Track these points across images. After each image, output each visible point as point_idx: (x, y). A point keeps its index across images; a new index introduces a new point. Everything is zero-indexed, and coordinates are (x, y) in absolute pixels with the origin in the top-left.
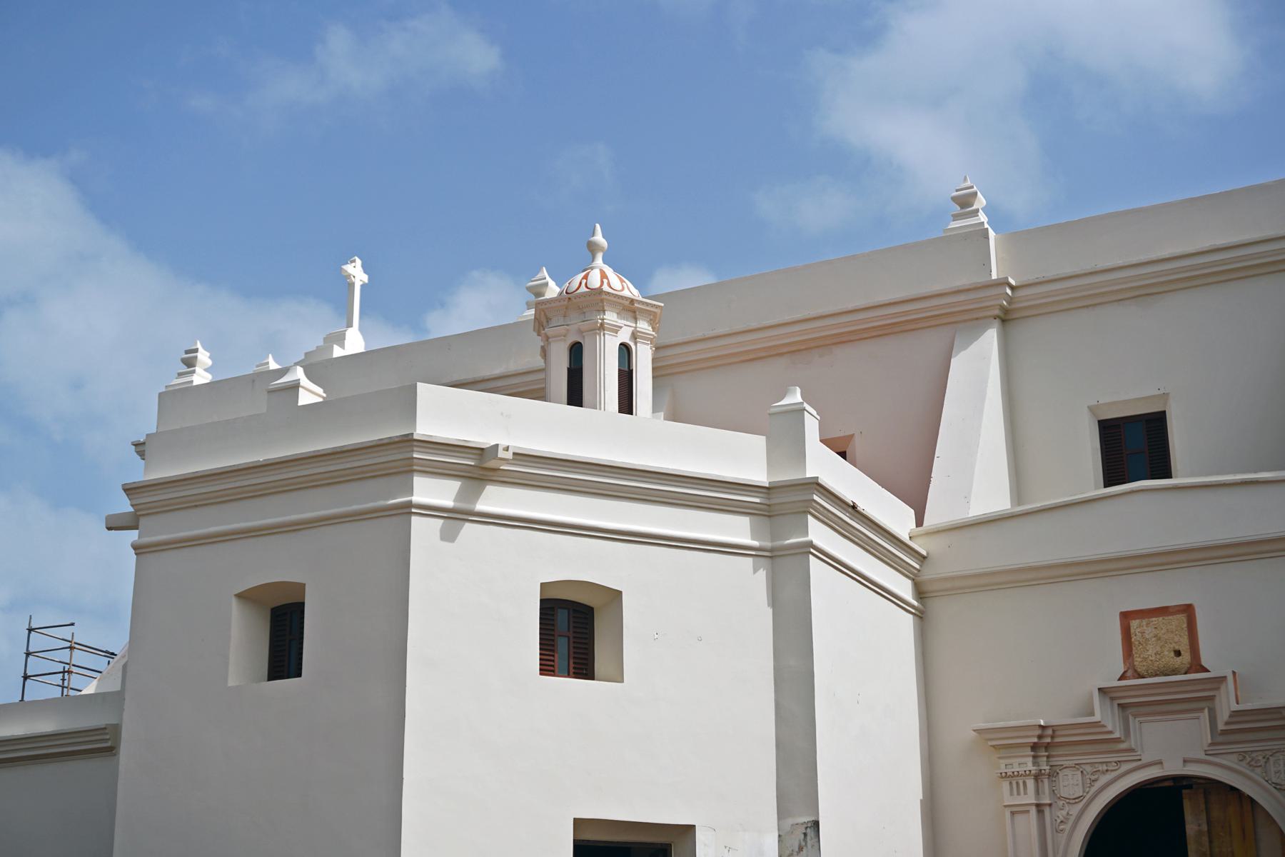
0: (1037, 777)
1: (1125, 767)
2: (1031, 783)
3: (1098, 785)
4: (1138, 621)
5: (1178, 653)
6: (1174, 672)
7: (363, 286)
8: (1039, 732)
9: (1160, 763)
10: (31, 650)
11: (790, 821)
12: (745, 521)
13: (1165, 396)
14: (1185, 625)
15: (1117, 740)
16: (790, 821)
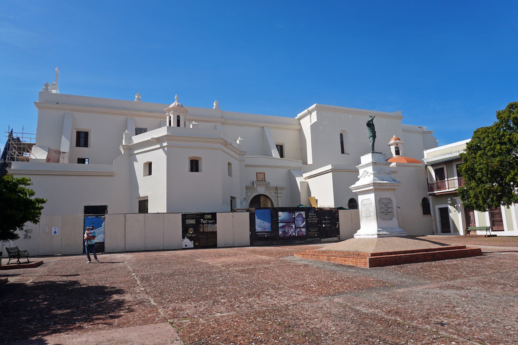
5: (263, 179)
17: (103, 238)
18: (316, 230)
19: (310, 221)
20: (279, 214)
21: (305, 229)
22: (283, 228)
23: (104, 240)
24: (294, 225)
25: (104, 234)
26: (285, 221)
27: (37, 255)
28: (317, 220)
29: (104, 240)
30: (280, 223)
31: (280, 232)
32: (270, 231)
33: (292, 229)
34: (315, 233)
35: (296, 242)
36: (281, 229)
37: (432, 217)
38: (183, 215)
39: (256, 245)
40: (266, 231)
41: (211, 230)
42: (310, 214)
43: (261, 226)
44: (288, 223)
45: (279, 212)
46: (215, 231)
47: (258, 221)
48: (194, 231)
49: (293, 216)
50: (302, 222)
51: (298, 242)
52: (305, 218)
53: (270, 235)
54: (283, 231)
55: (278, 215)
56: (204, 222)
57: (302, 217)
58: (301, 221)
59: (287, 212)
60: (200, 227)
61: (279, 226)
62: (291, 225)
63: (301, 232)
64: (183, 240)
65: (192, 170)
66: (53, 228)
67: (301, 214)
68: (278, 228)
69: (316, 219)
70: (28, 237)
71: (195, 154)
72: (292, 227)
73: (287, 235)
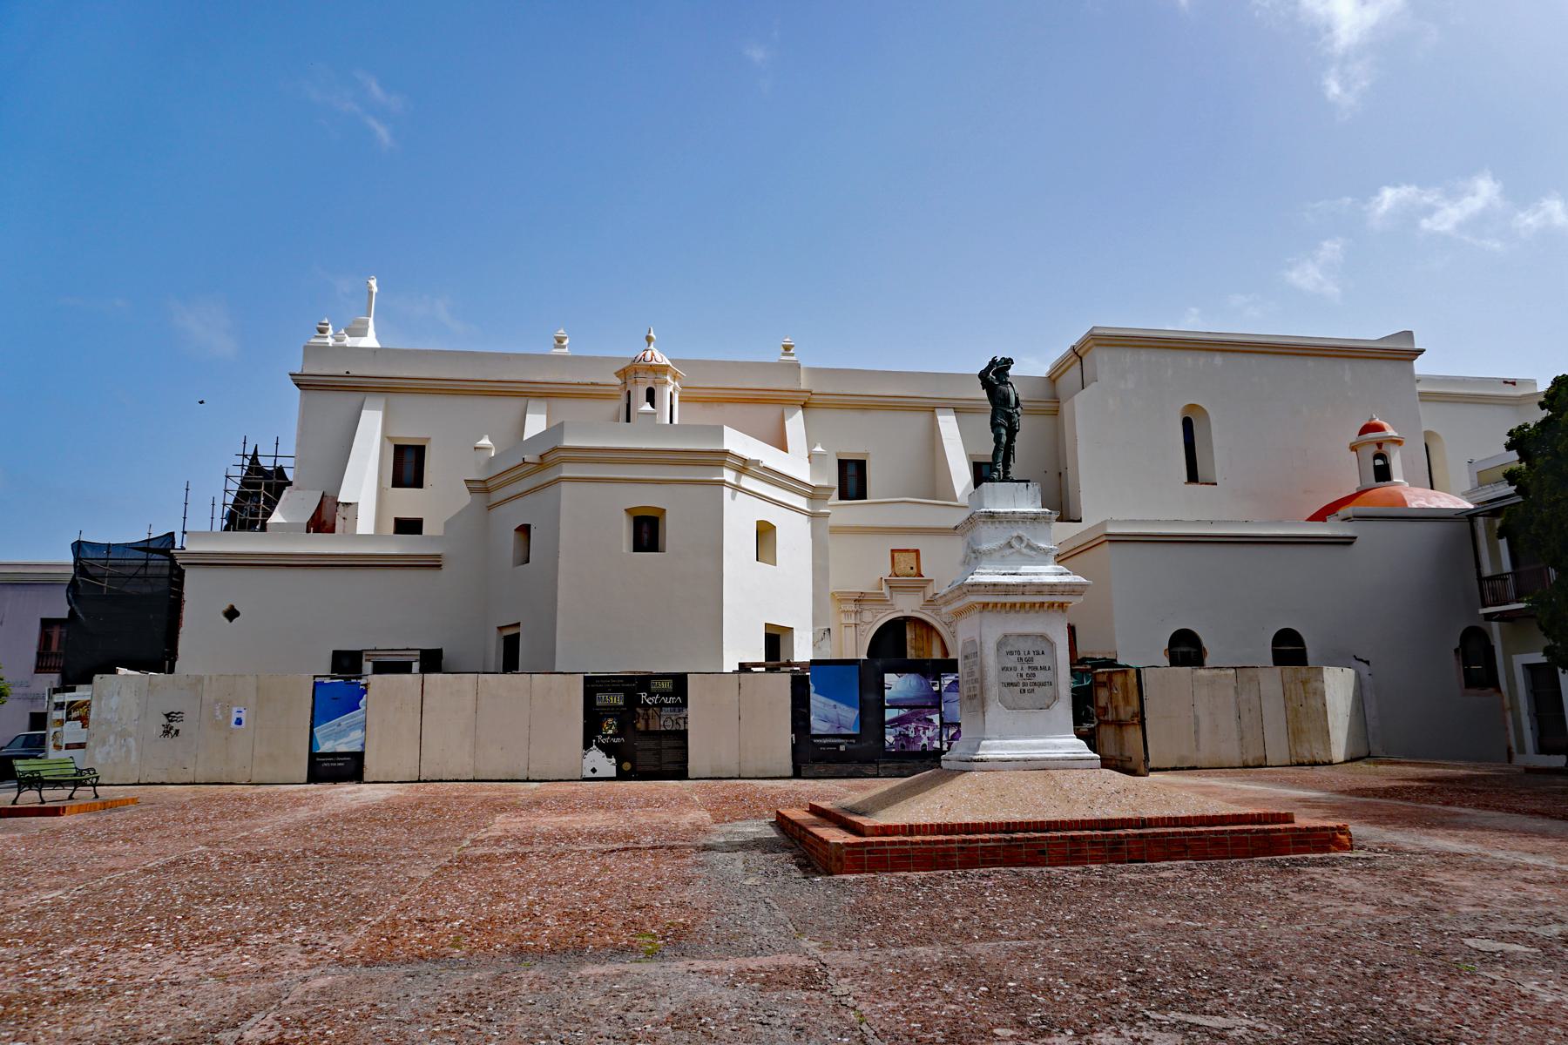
0: (856, 613)
1: (888, 611)
2: (853, 615)
3: (878, 618)
5: (912, 568)
6: (910, 576)
7: (376, 294)
9: (902, 611)
10: (228, 488)
11: (818, 628)
12: (805, 500)
15: (888, 601)
16: (818, 628)
17: (360, 742)
20: (886, 681)
22: (899, 725)
23: (363, 745)
25: (365, 729)
27: (193, 781)
29: (363, 745)
31: (887, 737)
32: (857, 732)
33: (931, 728)
36: (892, 727)
37: (1503, 697)
38: (587, 680)
39: (812, 775)
40: (845, 731)
41: (669, 726)
43: (826, 717)
45: (886, 675)
46: (682, 728)
47: (817, 702)
48: (617, 727)
49: (936, 688)
53: (854, 746)
54: (900, 734)
55: (884, 683)
56: (651, 701)
59: (913, 675)
60: (637, 716)
61: (887, 718)
64: (586, 754)
65: (638, 546)
66: (235, 709)
68: (882, 724)
70: (173, 732)
71: (647, 498)
72: (931, 721)
73: (914, 748)
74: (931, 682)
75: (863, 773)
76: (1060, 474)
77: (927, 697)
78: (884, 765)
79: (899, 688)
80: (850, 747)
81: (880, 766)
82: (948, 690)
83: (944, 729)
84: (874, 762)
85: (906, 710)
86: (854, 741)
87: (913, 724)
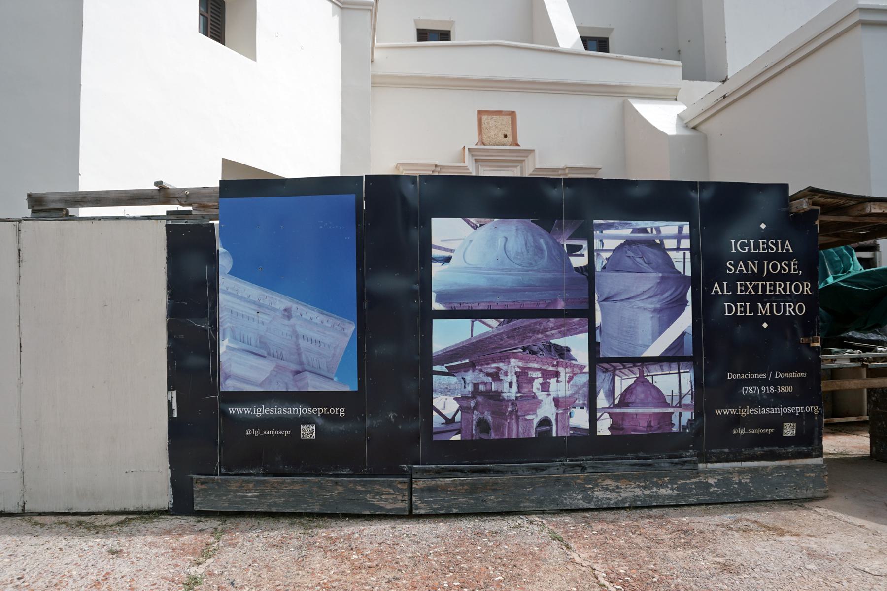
4: (486, 116)
5: (506, 136)
8: (433, 168)
13: (452, 23)
14: (510, 122)
18: (789, 389)
19: (738, 309)
20: (434, 241)
21: (688, 377)
22: (472, 366)
24: (585, 337)
26: (497, 303)
28: (802, 298)
30: (449, 315)
31: (438, 402)
32: (351, 386)
33: (564, 373)
34: (782, 410)
35: (599, 494)
36: (451, 372)
39: (223, 506)
40: (314, 384)
42: (735, 246)
43: (263, 344)
44: (525, 322)
49: (579, 261)
50: (655, 310)
51: (617, 490)
52: (694, 280)
53: (342, 427)
54: (476, 392)
57: (657, 269)
58: (655, 304)
62: (560, 342)
63: (644, 404)
67: (651, 243)
69: (791, 288)
72: (563, 353)
73: (514, 430)
74: (566, 243)
75: (366, 504)
76: (679, 51)
77: (553, 285)
78: (430, 482)
79: (474, 258)
80: (332, 427)
81: (419, 484)
82: (614, 265)
83: (602, 380)
84: (402, 474)
85: (493, 322)
86: (342, 413)
87: (514, 362)
